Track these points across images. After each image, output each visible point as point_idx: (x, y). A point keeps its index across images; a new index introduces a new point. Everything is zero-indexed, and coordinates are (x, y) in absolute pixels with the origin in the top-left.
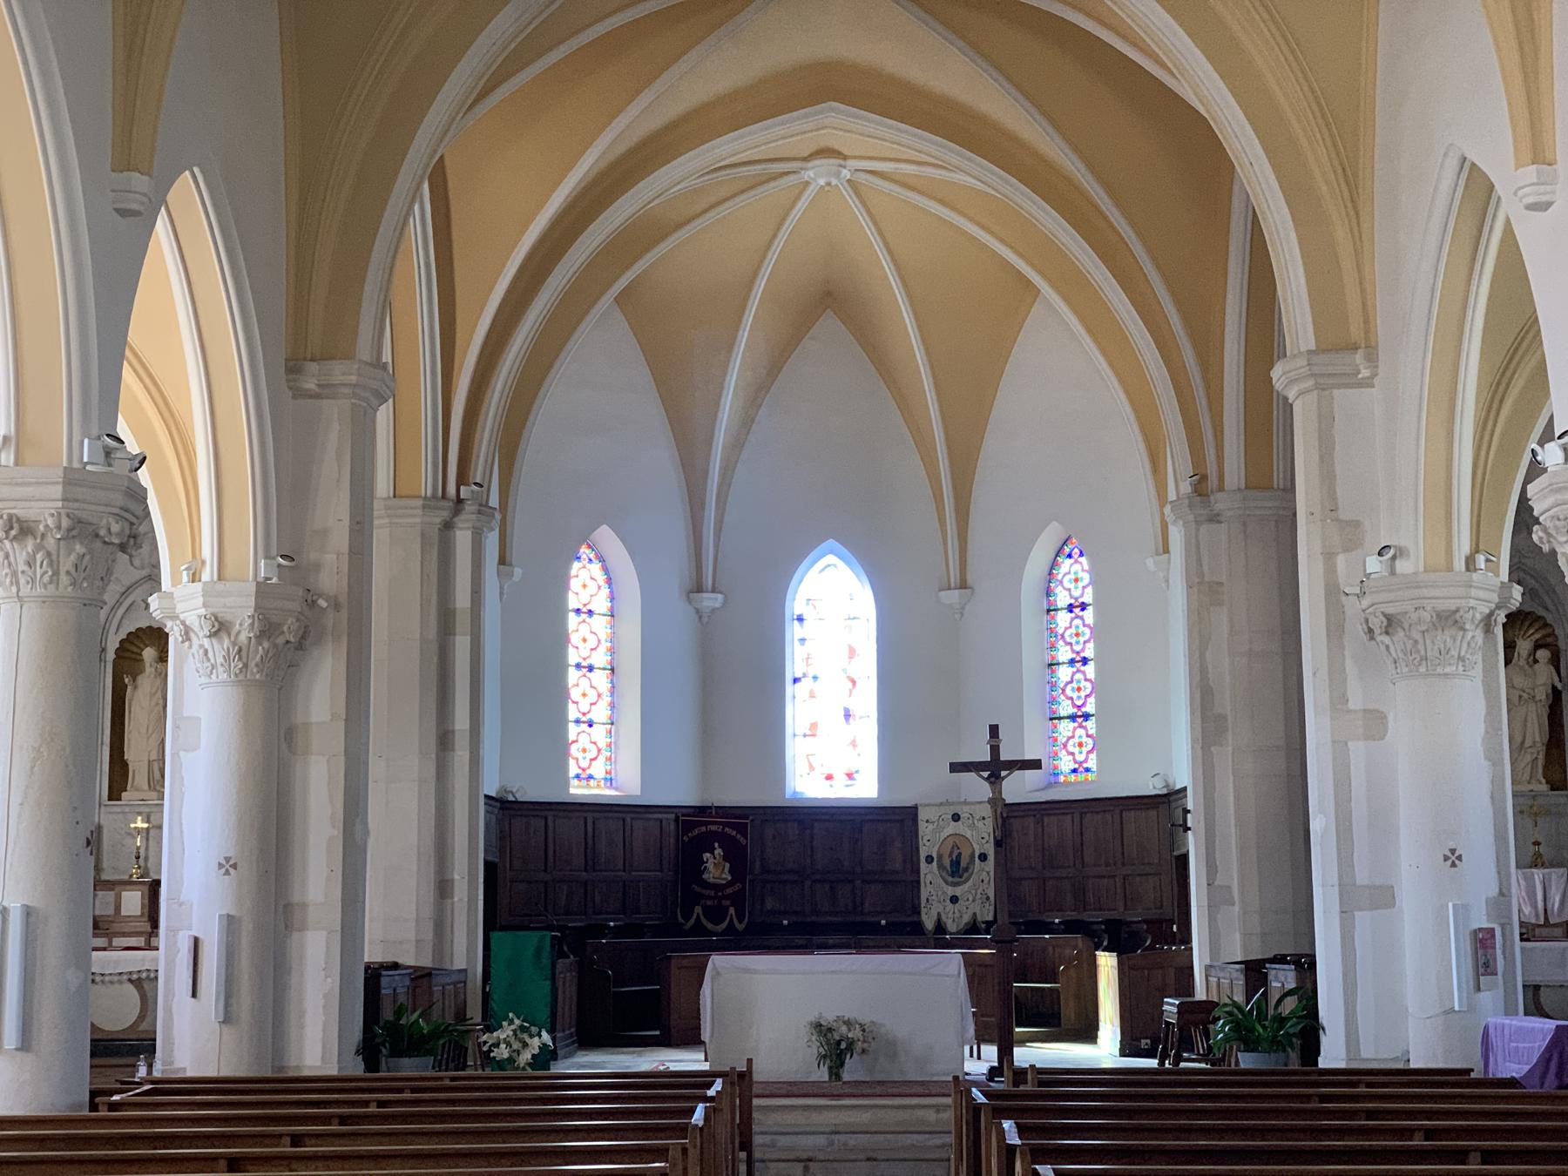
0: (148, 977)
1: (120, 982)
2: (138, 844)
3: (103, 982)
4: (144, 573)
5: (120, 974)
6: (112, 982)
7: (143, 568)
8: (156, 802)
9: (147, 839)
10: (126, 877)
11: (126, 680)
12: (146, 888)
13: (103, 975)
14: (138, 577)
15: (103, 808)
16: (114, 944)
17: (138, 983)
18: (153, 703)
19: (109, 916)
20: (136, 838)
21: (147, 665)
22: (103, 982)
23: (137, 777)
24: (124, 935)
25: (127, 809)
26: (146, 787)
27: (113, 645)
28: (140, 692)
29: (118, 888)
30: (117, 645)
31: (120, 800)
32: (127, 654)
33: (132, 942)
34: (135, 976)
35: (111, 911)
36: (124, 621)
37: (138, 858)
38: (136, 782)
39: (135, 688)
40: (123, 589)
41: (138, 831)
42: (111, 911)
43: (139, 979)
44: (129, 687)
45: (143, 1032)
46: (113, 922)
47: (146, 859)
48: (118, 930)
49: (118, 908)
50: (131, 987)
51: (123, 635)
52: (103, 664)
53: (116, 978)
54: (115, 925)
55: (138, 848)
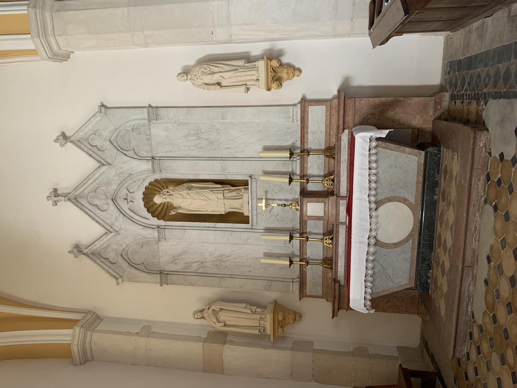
0: (375, 196)
1: (377, 217)
2: (276, 205)
3: (376, 230)
4: (111, 203)
5: (371, 217)
6: (377, 223)
7: (108, 204)
8: (250, 195)
9: (274, 199)
10: (298, 213)
11: (173, 213)
12: (305, 200)
13: (371, 230)
14: (114, 206)
15: (253, 227)
16: (344, 221)
17: (379, 204)
18: (188, 197)
19: (324, 224)
20: (273, 207)
21: (165, 201)
22: (376, 230)
23: (234, 207)
24: (337, 214)
25: (255, 212)
26: (240, 201)
27: (155, 221)
28: (183, 205)
29: (305, 218)
30: (156, 218)
31: (249, 216)
32: (163, 213)
33: (343, 209)
34: (373, 206)
35: (321, 223)
36: (141, 215)
37: (285, 205)
38: (238, 207)
39: (180, 207)
40: (122, 216)
41: (267, 205)
42: (321, 223)
43: (376, 202)
44: (179, 211)
45: (416, 200)
46: (328, 221)
47: (286, 200)
48: (334, 219)
49: (318, 218)
50: (383, 208)
51: (149, 215)
52: (167, 227)
53: (374, 220)
54: (330, 220)
55: (279, 205)
